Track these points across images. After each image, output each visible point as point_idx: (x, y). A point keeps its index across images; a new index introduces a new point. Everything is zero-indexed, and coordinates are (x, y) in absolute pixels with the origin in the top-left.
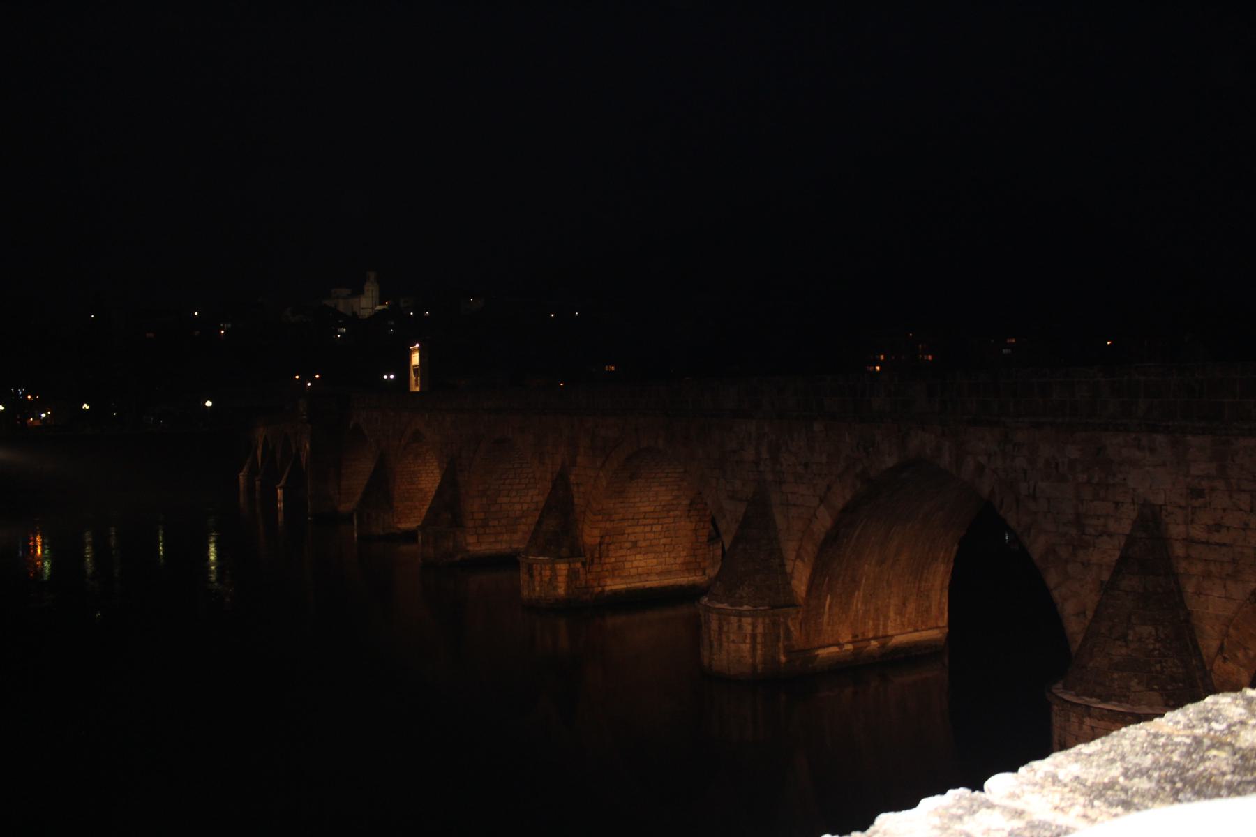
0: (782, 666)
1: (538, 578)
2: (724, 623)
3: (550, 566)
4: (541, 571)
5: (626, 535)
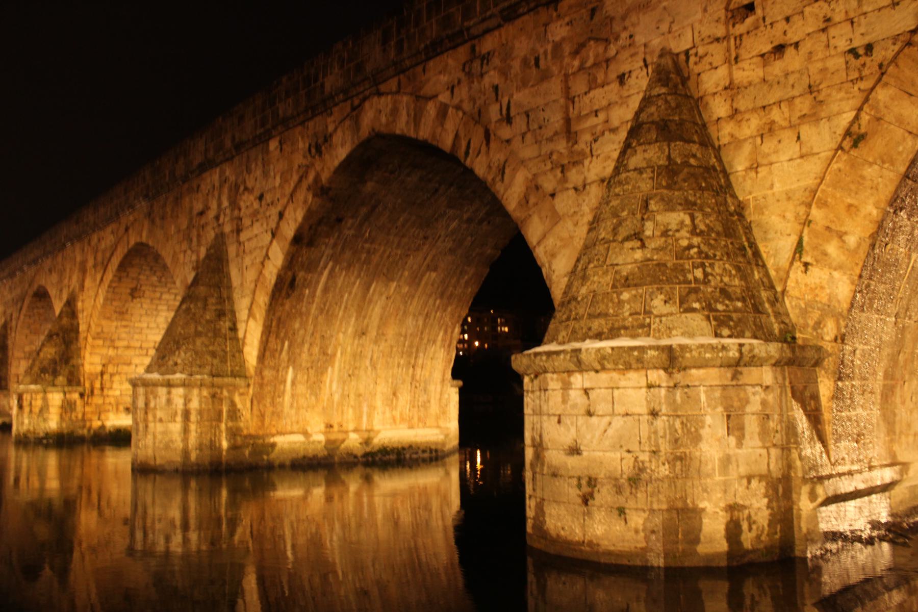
0: (224, 453)
1: (27, 409)
2: (151, 397)
5: (133, 367)
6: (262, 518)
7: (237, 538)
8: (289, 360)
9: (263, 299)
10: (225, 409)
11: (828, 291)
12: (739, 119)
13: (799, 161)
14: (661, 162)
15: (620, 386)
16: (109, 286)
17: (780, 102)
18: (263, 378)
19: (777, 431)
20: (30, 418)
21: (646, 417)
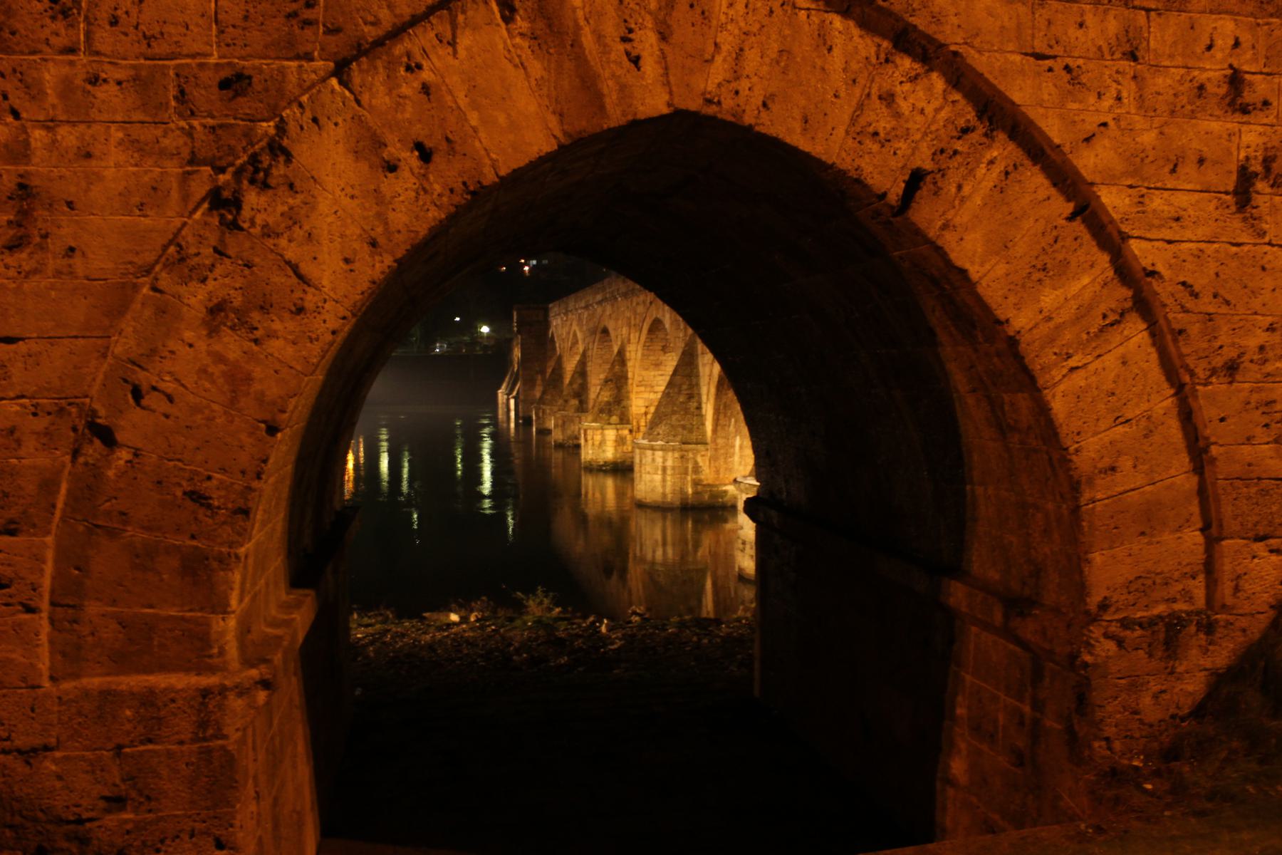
1: (590, 442)
3: (600, 431)
6: (718, 542)
7: (699, 554)
8: (736, 431)
9: (713, 390)
10: (690, 466)
16: (644, 346)
18: (717, 445)
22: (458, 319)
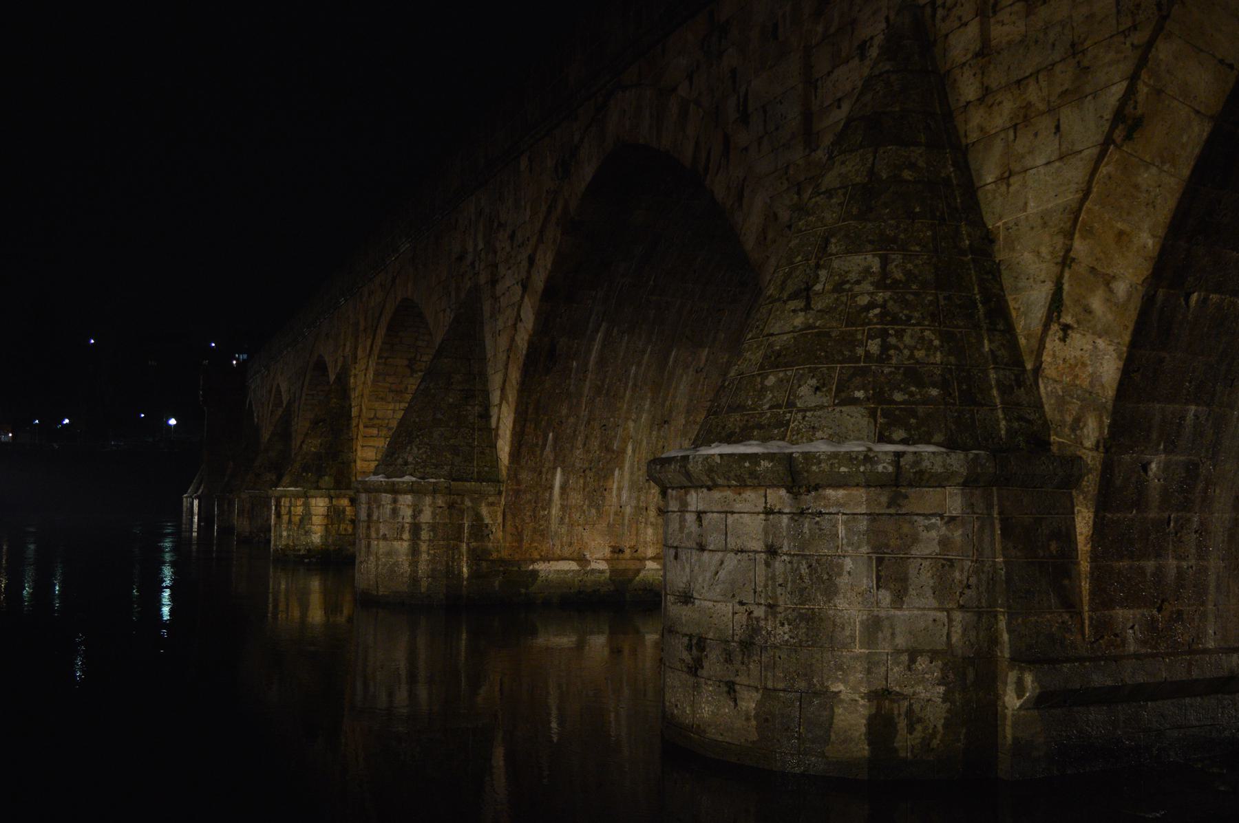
0: (465, 583)
1: (285, 518)
3: (303, 500)
4: (290, 507)
8: (555, 459)
9: (515, 375)
11: (1090, 369)
12: (990, 103)
13: (1057, 164)
14: (858, 180)
15: (736, 511)
16: (378, 359)
17: (1038, 72)
18: (519, 483)
19: (969, 587)
20: (288, 530)
21: (763, 556)
22: (143, 415)
